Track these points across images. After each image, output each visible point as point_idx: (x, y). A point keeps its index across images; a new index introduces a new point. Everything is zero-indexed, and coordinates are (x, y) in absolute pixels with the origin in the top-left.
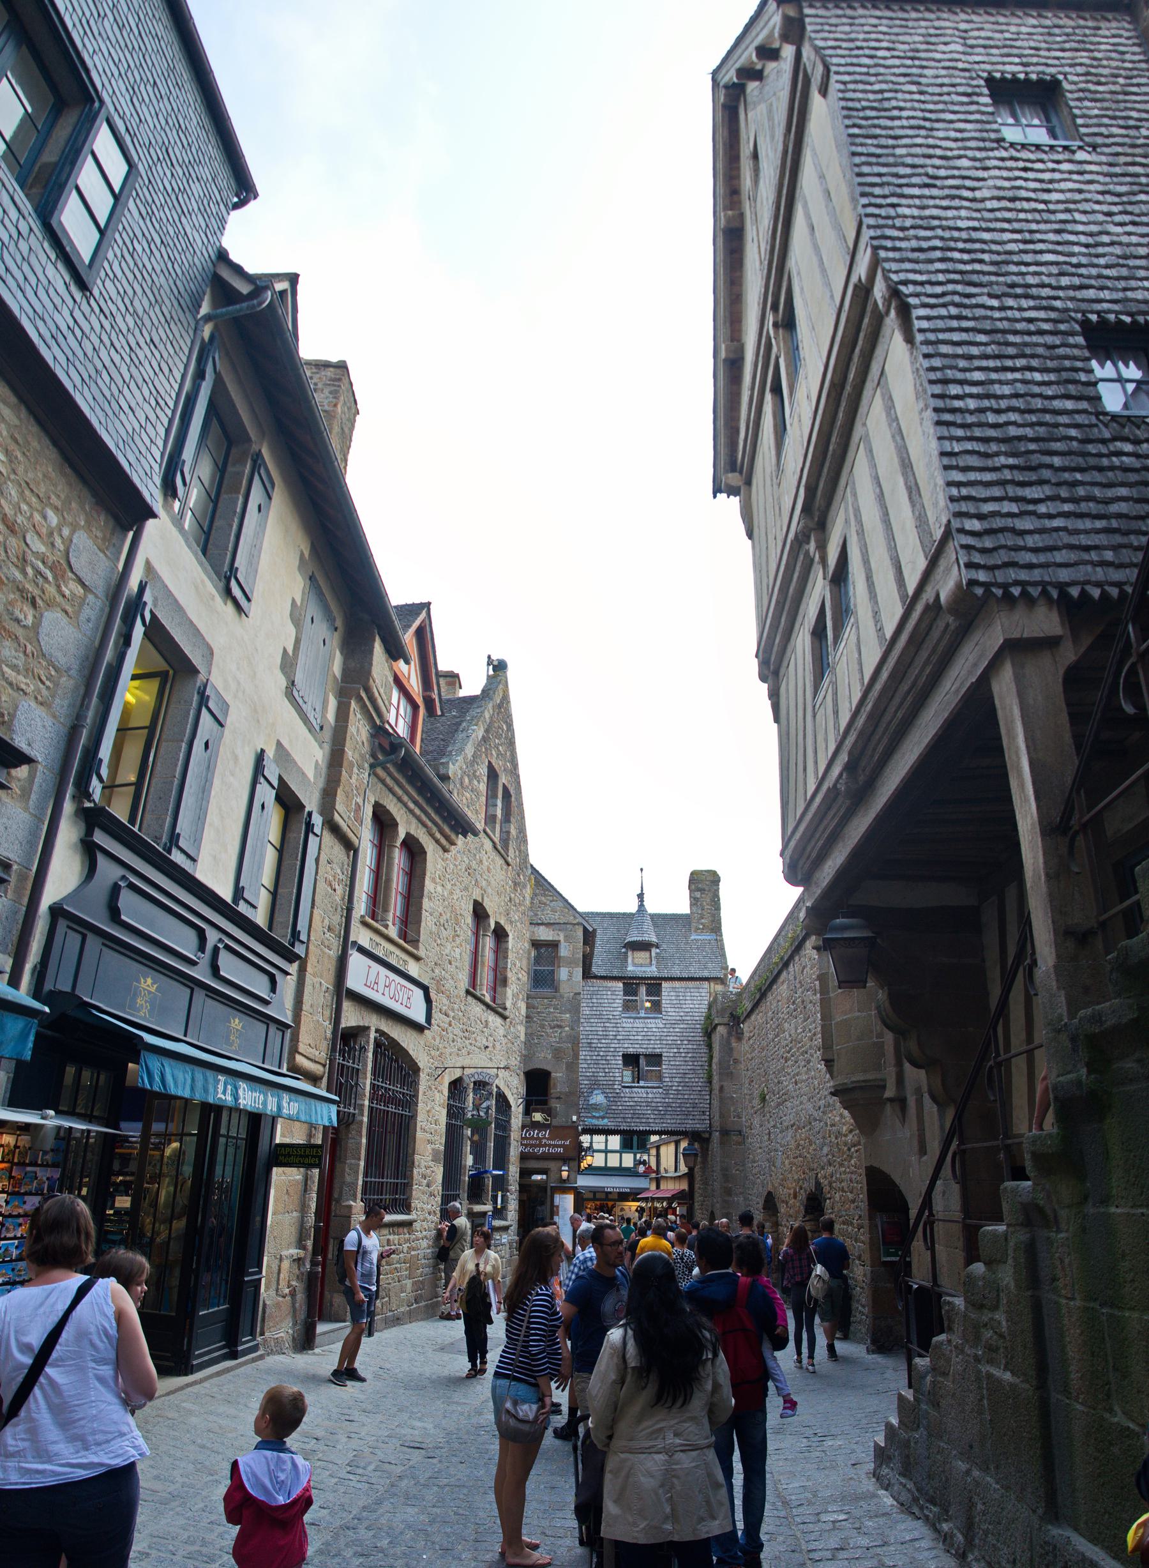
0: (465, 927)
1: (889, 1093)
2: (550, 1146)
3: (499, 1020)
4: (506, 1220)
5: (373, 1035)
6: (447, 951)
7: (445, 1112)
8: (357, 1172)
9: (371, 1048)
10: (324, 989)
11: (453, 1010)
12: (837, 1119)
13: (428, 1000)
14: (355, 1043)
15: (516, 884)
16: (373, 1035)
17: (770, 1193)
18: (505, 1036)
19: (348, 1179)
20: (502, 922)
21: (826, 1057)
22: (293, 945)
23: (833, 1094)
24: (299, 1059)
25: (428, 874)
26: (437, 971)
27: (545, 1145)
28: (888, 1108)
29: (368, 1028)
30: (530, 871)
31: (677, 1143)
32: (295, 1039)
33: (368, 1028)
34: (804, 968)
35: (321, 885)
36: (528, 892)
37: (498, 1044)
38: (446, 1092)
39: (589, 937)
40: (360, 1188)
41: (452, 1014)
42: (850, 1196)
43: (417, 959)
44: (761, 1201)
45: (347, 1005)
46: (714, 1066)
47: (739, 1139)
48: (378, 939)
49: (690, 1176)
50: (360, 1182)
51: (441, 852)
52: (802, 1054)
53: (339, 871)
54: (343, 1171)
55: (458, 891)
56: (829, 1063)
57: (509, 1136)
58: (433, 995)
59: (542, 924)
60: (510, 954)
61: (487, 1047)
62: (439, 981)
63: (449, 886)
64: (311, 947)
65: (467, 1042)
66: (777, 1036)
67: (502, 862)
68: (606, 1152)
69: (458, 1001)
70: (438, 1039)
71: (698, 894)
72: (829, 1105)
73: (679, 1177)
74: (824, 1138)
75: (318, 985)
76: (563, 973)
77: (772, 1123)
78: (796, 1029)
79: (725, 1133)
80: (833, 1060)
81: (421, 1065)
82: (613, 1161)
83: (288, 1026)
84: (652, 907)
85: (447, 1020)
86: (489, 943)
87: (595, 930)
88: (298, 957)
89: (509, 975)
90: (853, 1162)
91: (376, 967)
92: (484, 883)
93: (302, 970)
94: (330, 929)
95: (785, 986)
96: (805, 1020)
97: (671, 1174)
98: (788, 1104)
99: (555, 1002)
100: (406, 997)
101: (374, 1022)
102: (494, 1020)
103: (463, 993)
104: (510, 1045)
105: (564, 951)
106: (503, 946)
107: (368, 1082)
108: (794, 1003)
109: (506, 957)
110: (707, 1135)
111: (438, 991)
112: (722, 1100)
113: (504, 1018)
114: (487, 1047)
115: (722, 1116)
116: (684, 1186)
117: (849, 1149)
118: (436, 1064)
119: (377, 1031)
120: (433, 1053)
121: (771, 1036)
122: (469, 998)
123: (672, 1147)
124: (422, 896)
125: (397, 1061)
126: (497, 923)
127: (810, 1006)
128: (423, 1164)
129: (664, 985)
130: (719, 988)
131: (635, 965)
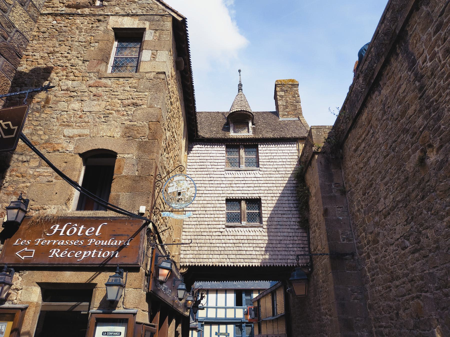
2: (99, 248)
27: (93, 247)
59: (128, 15)
68: (226, 308)
73: (277, 319)
82: (230, 314)
87: (184, 20)
131: (235, 132)
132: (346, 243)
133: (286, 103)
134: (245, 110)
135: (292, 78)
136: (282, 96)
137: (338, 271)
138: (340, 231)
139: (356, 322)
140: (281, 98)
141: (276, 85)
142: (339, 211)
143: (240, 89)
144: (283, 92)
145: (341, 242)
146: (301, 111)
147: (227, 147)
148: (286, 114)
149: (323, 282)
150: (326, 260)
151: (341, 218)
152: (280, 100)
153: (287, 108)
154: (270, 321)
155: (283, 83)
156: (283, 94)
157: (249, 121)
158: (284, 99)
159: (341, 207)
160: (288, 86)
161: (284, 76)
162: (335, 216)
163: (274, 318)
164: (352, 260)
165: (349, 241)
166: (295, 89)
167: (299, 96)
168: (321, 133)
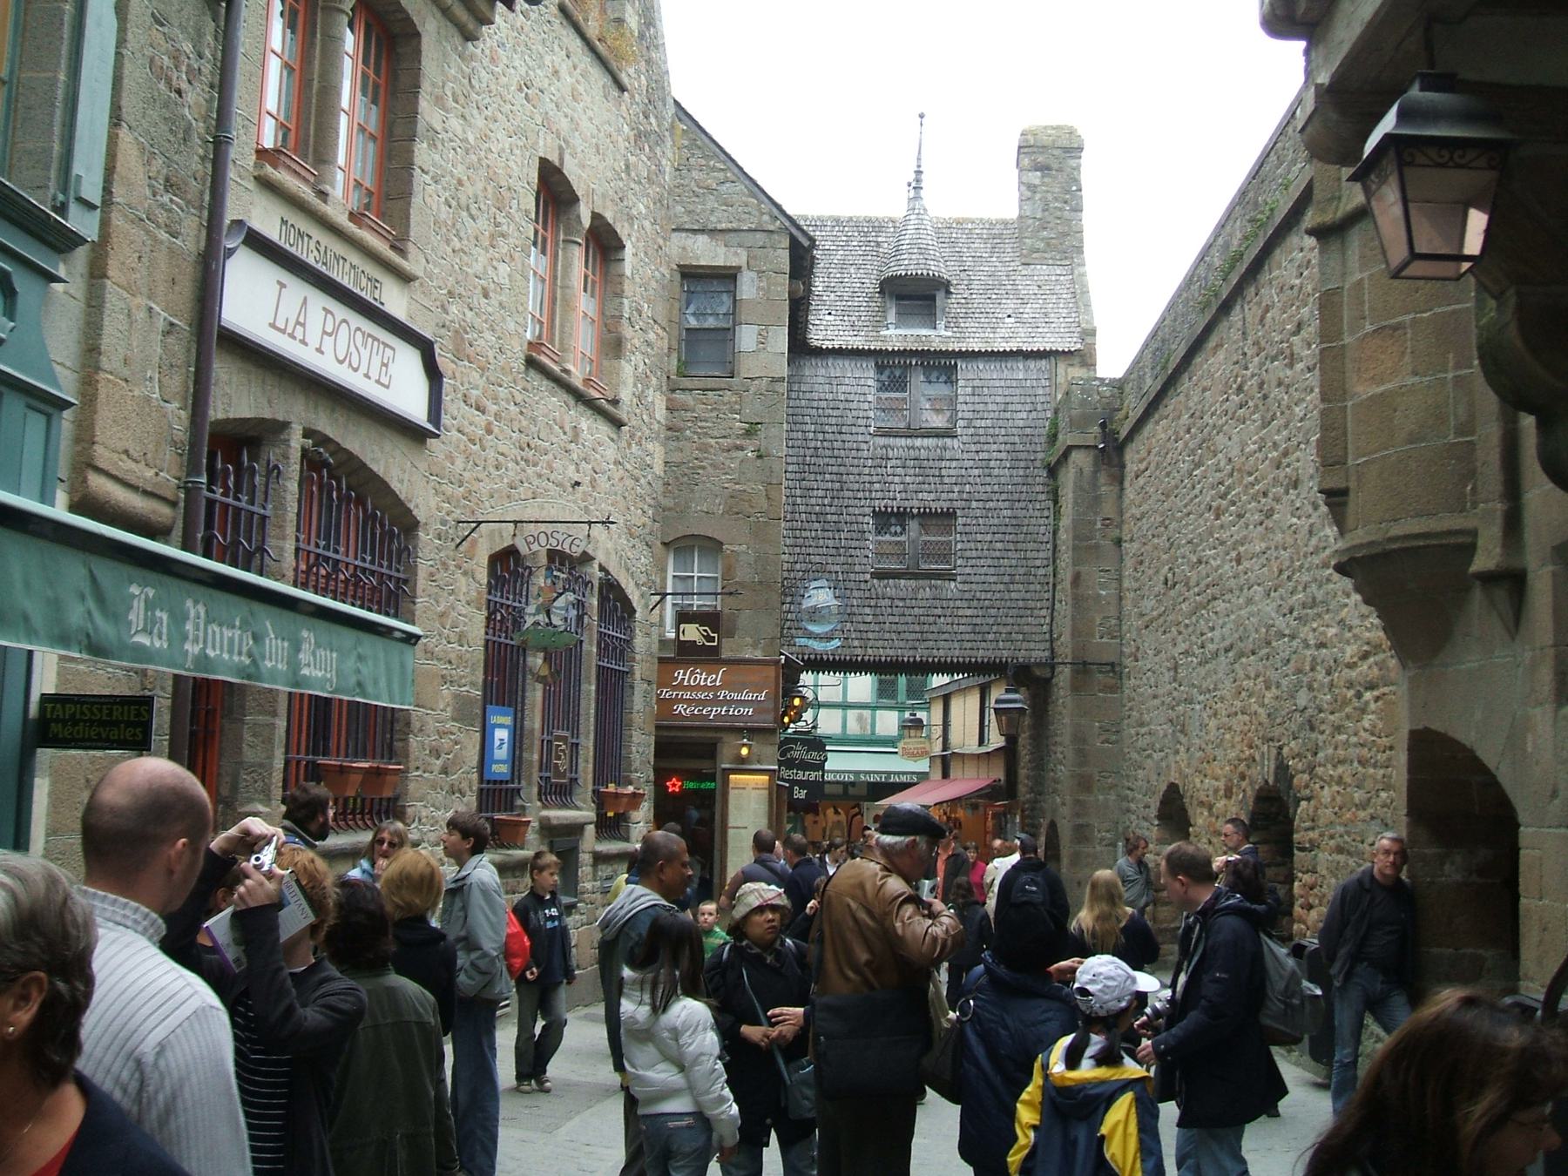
0: (518, 217)
1: (1484, 560)
3: (603, 429)
4: (627, 839)
5: (296, 441)
6: (478, 268)
7: (480, 617)
8: (269, 741)
9: (294, 469)
10: (161, 325)
11: (496, 400)
12: (1332, 631)
13: (433, 373)
14: (254, 457)
15: (640, 136)
16: (296, 441)
17: (1173, 789)
18: (617, 463)
19: (249, 755)
20: (609, 216)
21: (1334, 483)
22: (62, 209)
23: (1341, 569)
24: (97, 483)
25: (426, 86)
26: (453, 309)
28: (1477, 595)
29: (284, 426)
30: (671, 110)
31: (984, 691)
32: (85, 436)
33: (284, 426)
34: (1267, 310)
35: (134, 73)
36: (668, 155)
37: (602, 480)
38: (483, 576)
39: (802, 258)
40: (277, 777)
41: (493, 408)
42: (1358, 796)
43: (405, 278)
44: (1155, 803)
45: (224, 371)
46: (1063, 536)
47: (1109, 680)
48: (304, 225)
49: (1009, 753)
50: (279, 763)
51: (457, 40)
52: (1254, 498)
53: (187, 47)
54: (239, 738)
55: (501, 135)
56: (1336, 499)
57: (631, 673)
58: (444, 361)
59: (702, 231)
60: (628, 287)
61: (577, 484)
62: (459, 334)
63: (480, 122)
64: (117, 220)
65: (530, 470)
66: (1198, 465)
67: (607, 80)
69: (506, 379)
70: (460, 462)
71: (1035, 178)
72: (1314, 603)
74: (1299, 671)
75: (141, 315)
76: (747, 338)
77: (1182, 647)
78: (1243, 445)
79: (1082, 668)
80: (1344, 492)
81: (420, 514)
83: (64, 405)
84: (942, 204)
85: (481, 419)
86: (577, 260)
88: (78, 240)
89: (627, 332)
90: (1366, 724)
91: (298, 290)
92: (564, 124)
93: (97, 273)
94: (169, 185)
95: (1221, 355)
96: (1266, 424)
97: (972, 747)
98: (1220, 606)
99: (728, 396)
100: (376, 361)
101: (299, 414)
102: (592, 428)
103: (519, 364)
104: (629, 483)
105: (748, 287)
106: (613, 268)
107: (290, 546)
108: (1240, 389)
109: (619, 295)
110: (1046, 673)
111: (458, 356)
112: (1078, 601)
113: (617, 424)
114: (577, 484)
115: (1076, 633)
116: (998, 773)
117: (1359, 695)
118: (457, 514)
119: (308, 434)
120: (449, 489)
121: (1184, 467)
122: (532, 373)
123: (973, 700)
124: (412, 138)
125: (360, 501)
126: (596, 217)
127: (1276, 392)
128: (432, 725)
129: (965, 370)
130: (1077, 372)
133: (1044, 211)
136: (1035, 186)
141: (1020, 147)
144: (1038, 173)
146: (1081, 241)
150: (1067, 670)
154: (973, 756)
156: (1037, 182)
158: (1038, 196)
160: (1056, 152)
161: (1046, 115)
163: (983, 750)
166: (1073, 163)
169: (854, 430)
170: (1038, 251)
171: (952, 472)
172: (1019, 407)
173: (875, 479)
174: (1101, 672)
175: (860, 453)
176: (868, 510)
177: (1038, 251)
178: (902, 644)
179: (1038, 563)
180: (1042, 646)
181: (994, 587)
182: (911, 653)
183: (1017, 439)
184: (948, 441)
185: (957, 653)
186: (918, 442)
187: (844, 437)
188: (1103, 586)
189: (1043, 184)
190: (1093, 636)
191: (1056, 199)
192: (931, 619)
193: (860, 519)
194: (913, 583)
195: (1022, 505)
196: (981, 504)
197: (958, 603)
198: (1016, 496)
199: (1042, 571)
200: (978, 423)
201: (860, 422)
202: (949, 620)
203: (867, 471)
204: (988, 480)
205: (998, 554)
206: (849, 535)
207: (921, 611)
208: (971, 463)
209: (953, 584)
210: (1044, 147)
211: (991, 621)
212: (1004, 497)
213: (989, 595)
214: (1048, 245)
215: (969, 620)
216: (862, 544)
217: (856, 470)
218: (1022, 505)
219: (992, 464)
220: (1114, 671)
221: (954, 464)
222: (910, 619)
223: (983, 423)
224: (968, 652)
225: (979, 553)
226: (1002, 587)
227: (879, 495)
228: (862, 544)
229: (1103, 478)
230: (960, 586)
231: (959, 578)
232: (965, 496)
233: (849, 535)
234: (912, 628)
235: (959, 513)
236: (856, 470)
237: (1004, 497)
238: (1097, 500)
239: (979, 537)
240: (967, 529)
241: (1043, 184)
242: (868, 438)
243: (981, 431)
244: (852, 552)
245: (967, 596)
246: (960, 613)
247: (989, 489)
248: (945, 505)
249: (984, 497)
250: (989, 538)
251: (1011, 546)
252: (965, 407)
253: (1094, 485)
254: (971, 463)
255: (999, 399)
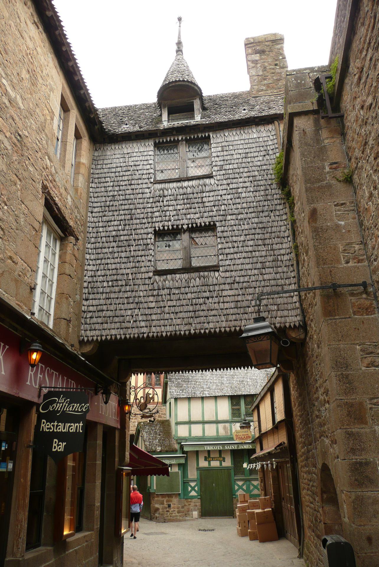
71: (257, 57)
132: (355, 267)
134: (181, 79)
135: (274, 32)
136: (257, 61)
137: (337, 317)
138: (341, 248)
139: (371, 408)
140: (253, 65)
142: (339, 210)
143: (179, 51)
144: (258, 55)
145: (342, 264)
147: (158, 146)
148: (264, 88)
149: (318, 347)
151: (343, 223)
152: (253, 67)
153: (265, 79)
155: (260, 40)
156: (257, 58)
157: (194, 101)
158: (259, 65)
159: (342, 204)
160: (267, 43)
162: (331, 220)
164: (364, 296)
165: (358, 262)
166: (279, 46)
167: (284, 58)
168: (304, 80)
169: (140, 182)
170: (262, 90)
171: (211, 199)
172: (256, 154)
173: (155, 209)
174: (352, 294)
175: (145, 195)
176: (150, 230)
177: (262, 90)
178: (179, 321)
179: (283, 252)
180: (294, 313)
181: (249, 272)
182: (187, 328)
183: (256, 173)
184: (207, 181)
185: (224, 324)
186: (186, 184)
187: (133, 187)
188: (340, 217)
189: (261, 59)
190: (338, 261)
191: (270, 65)
192: (201, 301)
193: (145, 236)
194: (185, 276)
195: (266, 214)
196: (234, 217)
197: (222, 287)
198: (260, 209)
199: (286, 257)
200: (227, 167)
201: (144, 176)
202: (216, 300)
203: (149, 205)
204: (238, 201)
205: (250, 249)
206: (137, 248)
207: (193, 296)
208: (225, 192)
209: (217, 274)
210: (259, 42)
211: (250, 297)
212: (251, 210)
213: (246, 279)
214: (268, 87)
215: (232, 299)
216: (147, 253)
217: (141, 206)
218: (266, 214)
219: (240, 190)
220: (366, 292)
221: (212, 194)
222: (184, 302)
223: (231, 167)
224: (233, 323)
225: (236, 250)
226: (256, 272)
227: (159, 219)
228: (147, 253)
229: (324, 134)
230: (223, 275)
231: (221, 269)
232: (222, 213)
233: (137, 248)
234: (186, 308)
235: (218, 224)
236: (141, 206)
237: (251, 210)
238: (322, 150)
239: (234, 239)
240: (225, 234)
241: (261, 59)
242: (150, 185)
243: (230, 171)
244: (139, 259)
245: (229, 280)
246: (225, 293)
247: (239, 206)
248: (207, 221)
249: (236, 212)
250: (242, 238)
251: (260, 242)
252: (217, 159)
253: (318, 141)
254: (225, 192)
255: (240, 151)
